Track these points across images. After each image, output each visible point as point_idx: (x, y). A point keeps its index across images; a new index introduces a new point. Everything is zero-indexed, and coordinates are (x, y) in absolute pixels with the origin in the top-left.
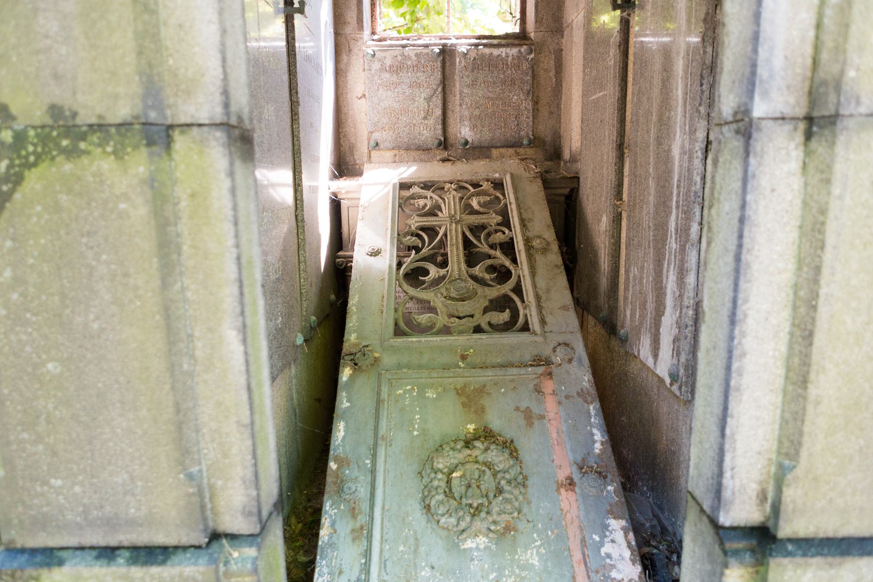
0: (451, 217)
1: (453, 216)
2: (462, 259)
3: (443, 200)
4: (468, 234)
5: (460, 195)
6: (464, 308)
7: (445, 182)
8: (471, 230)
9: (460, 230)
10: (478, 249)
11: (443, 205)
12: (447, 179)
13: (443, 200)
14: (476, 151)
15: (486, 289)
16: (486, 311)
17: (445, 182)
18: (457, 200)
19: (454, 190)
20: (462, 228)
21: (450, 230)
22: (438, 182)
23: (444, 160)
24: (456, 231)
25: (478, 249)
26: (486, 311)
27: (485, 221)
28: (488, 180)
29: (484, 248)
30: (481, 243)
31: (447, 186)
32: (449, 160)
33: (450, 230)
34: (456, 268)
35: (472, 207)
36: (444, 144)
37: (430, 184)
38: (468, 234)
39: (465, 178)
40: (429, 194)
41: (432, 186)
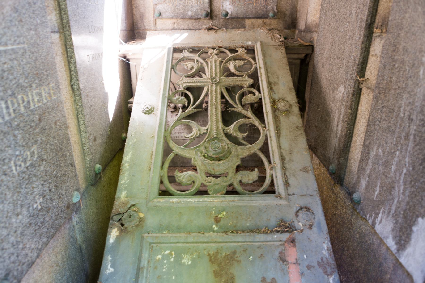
0: (213, 79)
1: (214, 78)
2: (220, 119)
3: (207, 62)
4: (226, 94)
5: (220, 59)
6: (219, 167)
7: (209, 48)
8: (228, 90)
9: (219, 91)
10: (233, 109)
11: (206, 68)
12: (211, 45)
13: (207, 62)
14: (235, 22)
15: (239, 147)
16: (238, 169)
17: (209, 48)
18: (218, 64)
19: (216, 55)
20: (221, 89)
21: (211, 91)
22: (204, 47)
23: (209, 29)
24: (216, 92)
25: (233, 109)
26: (238, 169)
27: (239, 83)
28: (242, 47)
29: (238, 108)
30: (236, 103)
31: (211, 51)
32: (212, 29)
33: (211, 91)
34: (214, 127)
35: (229, 70)
36: (210, 15)
37: (197, 49)
38: (226, 94)
39: (225, 44)
40: (195, 57)
41: (199, 51)
